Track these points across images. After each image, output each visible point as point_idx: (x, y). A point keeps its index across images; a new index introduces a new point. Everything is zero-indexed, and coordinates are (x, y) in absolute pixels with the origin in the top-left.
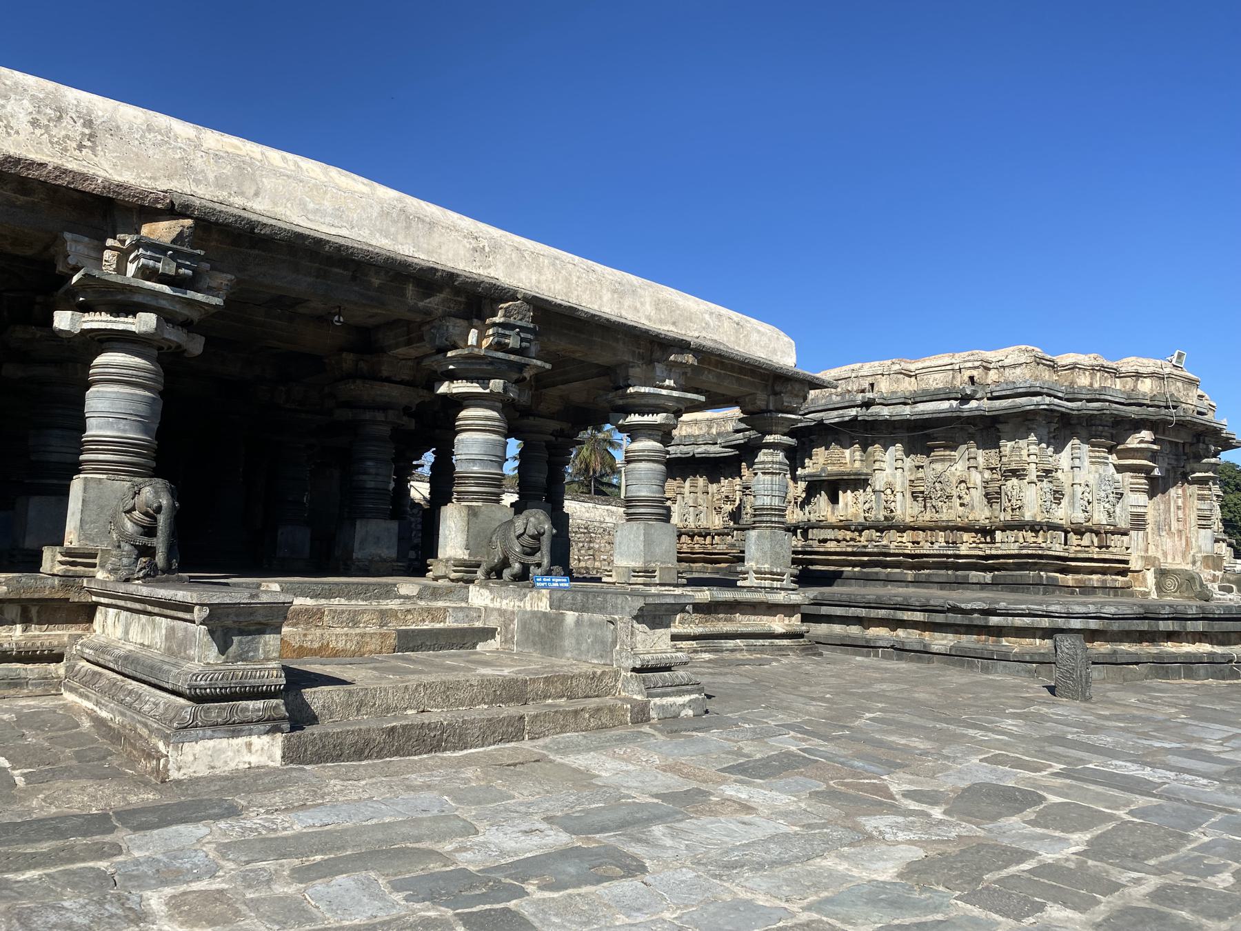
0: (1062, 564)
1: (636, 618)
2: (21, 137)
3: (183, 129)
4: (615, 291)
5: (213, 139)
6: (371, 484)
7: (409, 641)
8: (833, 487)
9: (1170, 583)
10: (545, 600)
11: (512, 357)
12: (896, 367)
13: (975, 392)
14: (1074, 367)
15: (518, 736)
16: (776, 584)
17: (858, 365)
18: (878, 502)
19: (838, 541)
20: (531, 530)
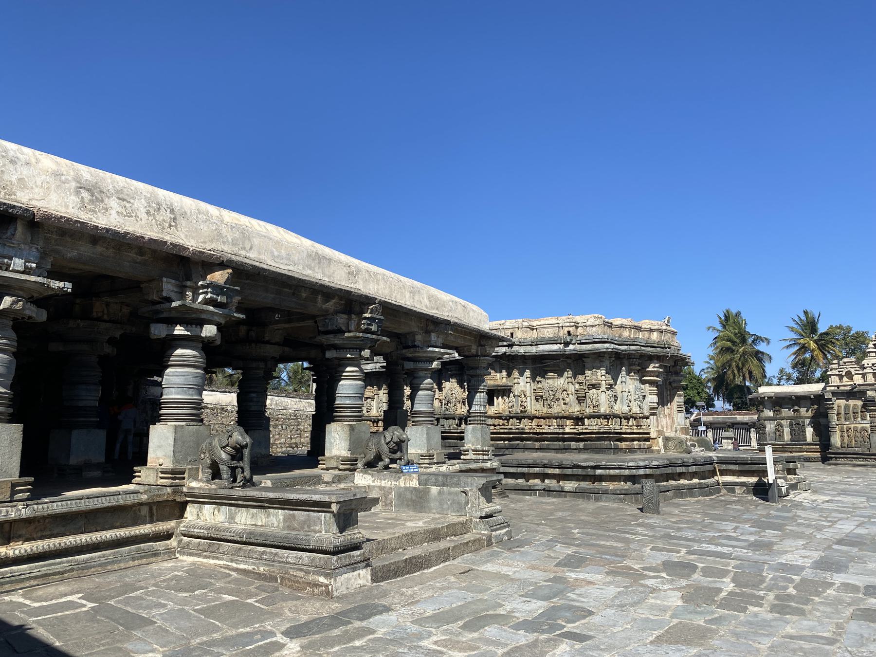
0: (619, 437)
2: (143, 222)
3: (213, 210)
4: (411, 292)
5: (230, 216)
6: (253, 408)
9: (671, 444)
10: (414, 480)
11: (374, 336)
12: (526, 324)
13: (571, 340)
14: (621, 326)
16: (486, 457)
17: (503, 321)
19: (495, 426)
20: (395, 439)
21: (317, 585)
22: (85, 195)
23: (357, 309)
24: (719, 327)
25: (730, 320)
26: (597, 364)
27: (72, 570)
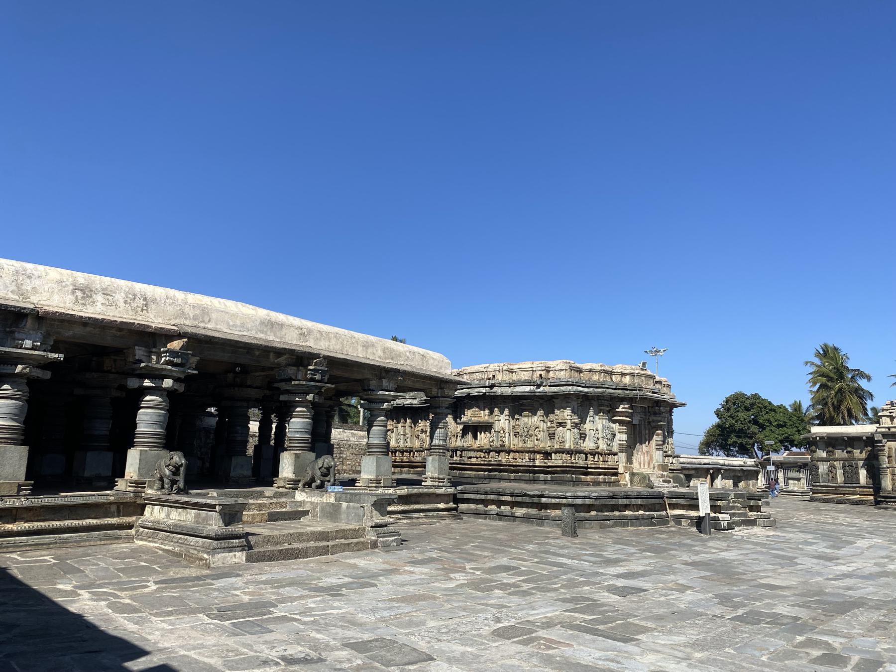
0: (585, 471)
1: (373, 505)
3: (179, 295)
4: (364, 346)
5: (194, 298)
6: (239, 439)
7: (273, 517)
8: (473, 429)
9: (636, 479)
11: (317, 384)
12: (505, 368)
14: (590, 371)
15: (326, 553)
18: (497, 436)
20: (325, 466)
21: (201, 559)
22: (79, 294)
23: (306, 362)
24: (817, 361)
25: (828, 353)
26: (564, 405)
27: (56, 543)
